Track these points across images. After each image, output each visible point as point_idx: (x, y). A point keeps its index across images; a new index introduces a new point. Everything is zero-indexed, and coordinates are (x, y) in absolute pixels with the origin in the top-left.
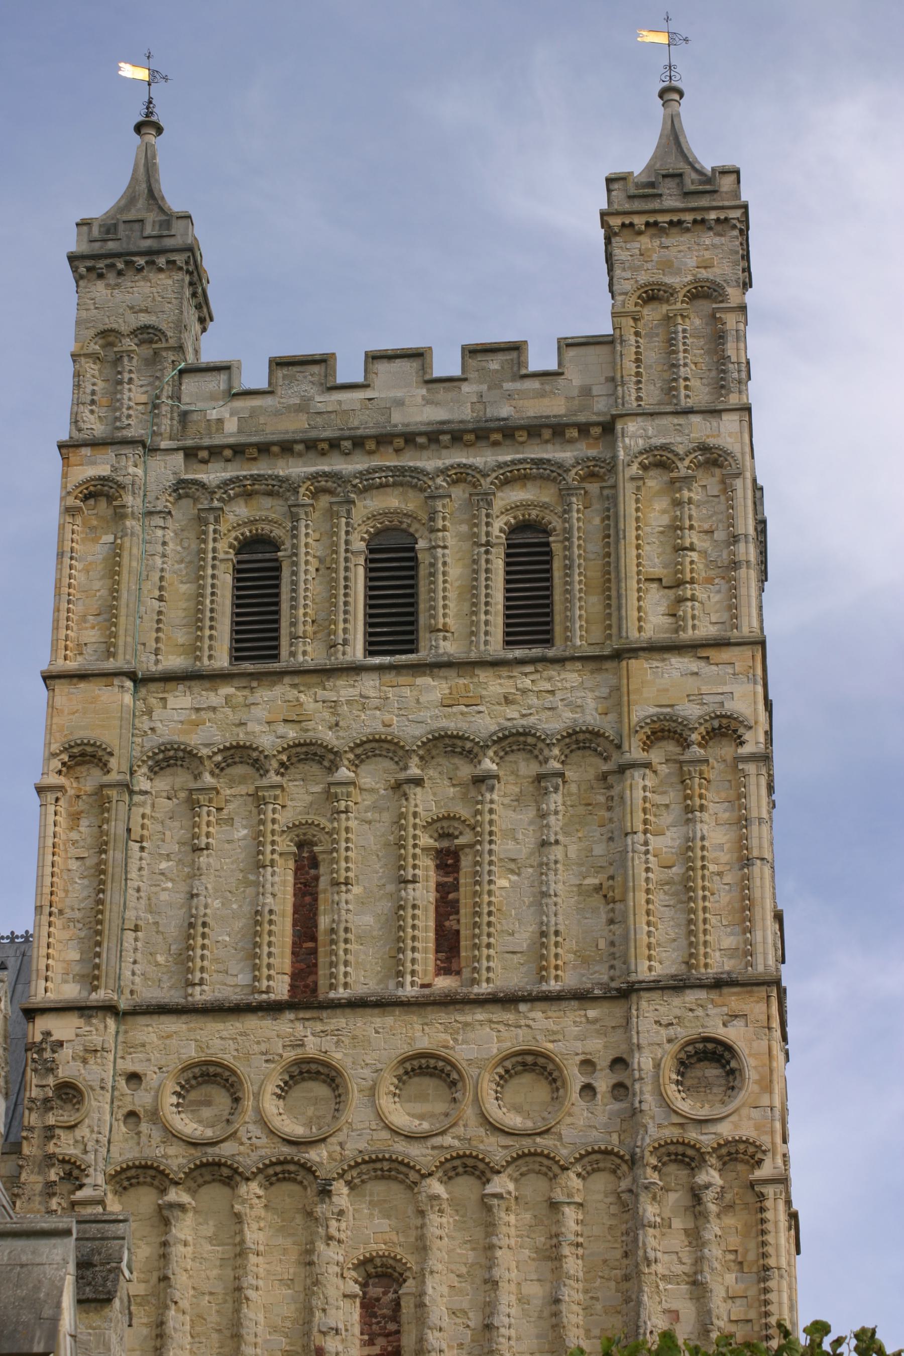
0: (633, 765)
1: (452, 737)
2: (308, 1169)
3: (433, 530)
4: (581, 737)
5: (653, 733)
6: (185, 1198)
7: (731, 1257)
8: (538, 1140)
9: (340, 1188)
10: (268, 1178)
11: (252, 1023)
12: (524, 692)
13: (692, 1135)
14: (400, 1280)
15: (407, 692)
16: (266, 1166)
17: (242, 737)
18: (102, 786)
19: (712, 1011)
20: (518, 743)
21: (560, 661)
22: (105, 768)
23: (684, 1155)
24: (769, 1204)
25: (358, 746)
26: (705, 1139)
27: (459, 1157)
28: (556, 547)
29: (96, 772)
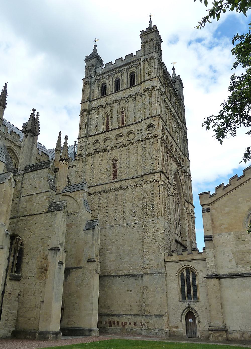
0: (142, 95)
11: (101, 135)
19: (152, 120)
21: (135, 86)
28: (135, 74)
29: (86, 112)
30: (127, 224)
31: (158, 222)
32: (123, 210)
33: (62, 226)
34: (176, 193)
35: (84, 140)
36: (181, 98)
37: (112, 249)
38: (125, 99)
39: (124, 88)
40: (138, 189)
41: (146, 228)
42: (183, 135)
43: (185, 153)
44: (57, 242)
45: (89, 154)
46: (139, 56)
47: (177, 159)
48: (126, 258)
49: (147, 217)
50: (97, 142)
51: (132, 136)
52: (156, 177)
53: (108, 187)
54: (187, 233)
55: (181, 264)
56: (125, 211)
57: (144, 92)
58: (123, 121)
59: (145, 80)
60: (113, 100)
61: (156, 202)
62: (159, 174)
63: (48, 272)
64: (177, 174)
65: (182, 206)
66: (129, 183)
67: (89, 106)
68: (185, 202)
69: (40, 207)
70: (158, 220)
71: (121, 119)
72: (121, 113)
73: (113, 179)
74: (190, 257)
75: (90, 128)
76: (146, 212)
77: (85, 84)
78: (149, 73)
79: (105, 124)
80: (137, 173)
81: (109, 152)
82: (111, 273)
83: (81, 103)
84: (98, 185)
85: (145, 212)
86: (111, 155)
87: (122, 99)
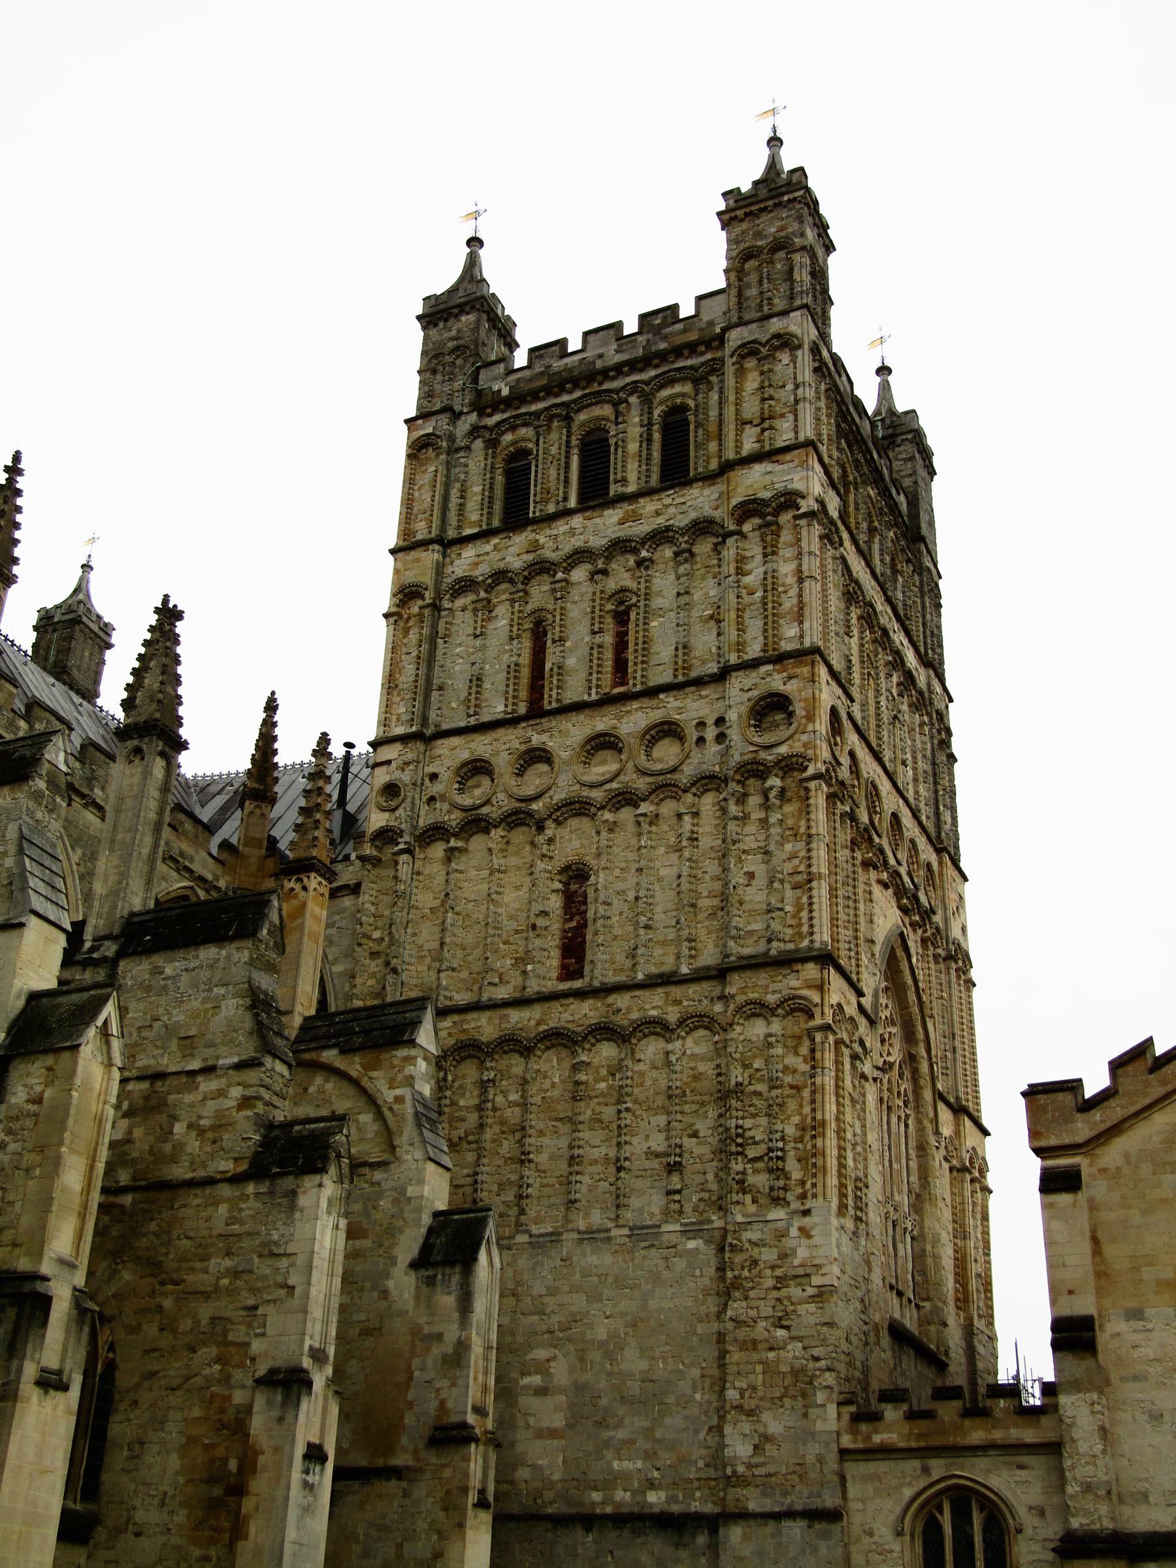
0: (731, 534)
1: (623, 541)
2: (530, 814)
3: (617, 424)
4: (701, 526)
5: (744, 513)
6: (460, 844)
7: (788, 833)
8: (669, 776)
9: (549, 824)
10: (508, 824)
11: (501, 732)
12: (667, 506)
13: (763, 755)
14: (587, 878)
15: (597, 520)
16: (506, 817)
17: (502, 565)
18: (420, 608)
19: (776, 676)
20: (663, 537)
21: (688, 483)
22: (422, 597)
23: (758, 770)
24: (813, 793)
25: (568, 558)
26: (768, 757)
27: (620, 794)
28: (691, 418)
29: (420, 603)
30: (643, 1234)
31: (805, 1232)
32: (612, 1153)
33: (326, 1254)
34: (891, 1059)
35: (412, 751)
36: (924, 530)
37: (552, 1364)
38: (635, 551)
39: (631, 488)
40: (696, 1044)
41: (739, 1258)
42: (932, 737)
43: (939, 836)
44: (302, 1341)
45: (436, 833)
46: (711, 323)
47: (903, 871)
48: (627, 1421)
49: (748, 1198)
50: (477, 768)
51: (667, 753)
52: (794, 983)
53: (533, 1023)
54: (950, 1284)
55: (926, 1470)
56: (626, 1159)
57: (740, 521)
58: (621, 666)
59: (744, 453)
60: (567, 548)
61: (796, 1119)
62: (811, 970)
63: (248, 1504)
64: (900, 953)
65: (921, 1129)
66: (653, 1004)
67: (439, 569)
68: (941, 1106)
69: (208, 1149)
70: (807, 1219)
71: (609, 655)
72: (609, 620)
73: (561, 979)
74: (977, 1435)
75: (441, 688)
76: (744, 1173)
77: (420, 449)
78: (766, 420)
79: (525, 673)
80: (693, 952)
81: (541, 828)
82: (539, 1501)
83: (393, 552)
84: (476, 1007)
85: (738, 1173)
86: (552, 848)
87: (620, 546)
